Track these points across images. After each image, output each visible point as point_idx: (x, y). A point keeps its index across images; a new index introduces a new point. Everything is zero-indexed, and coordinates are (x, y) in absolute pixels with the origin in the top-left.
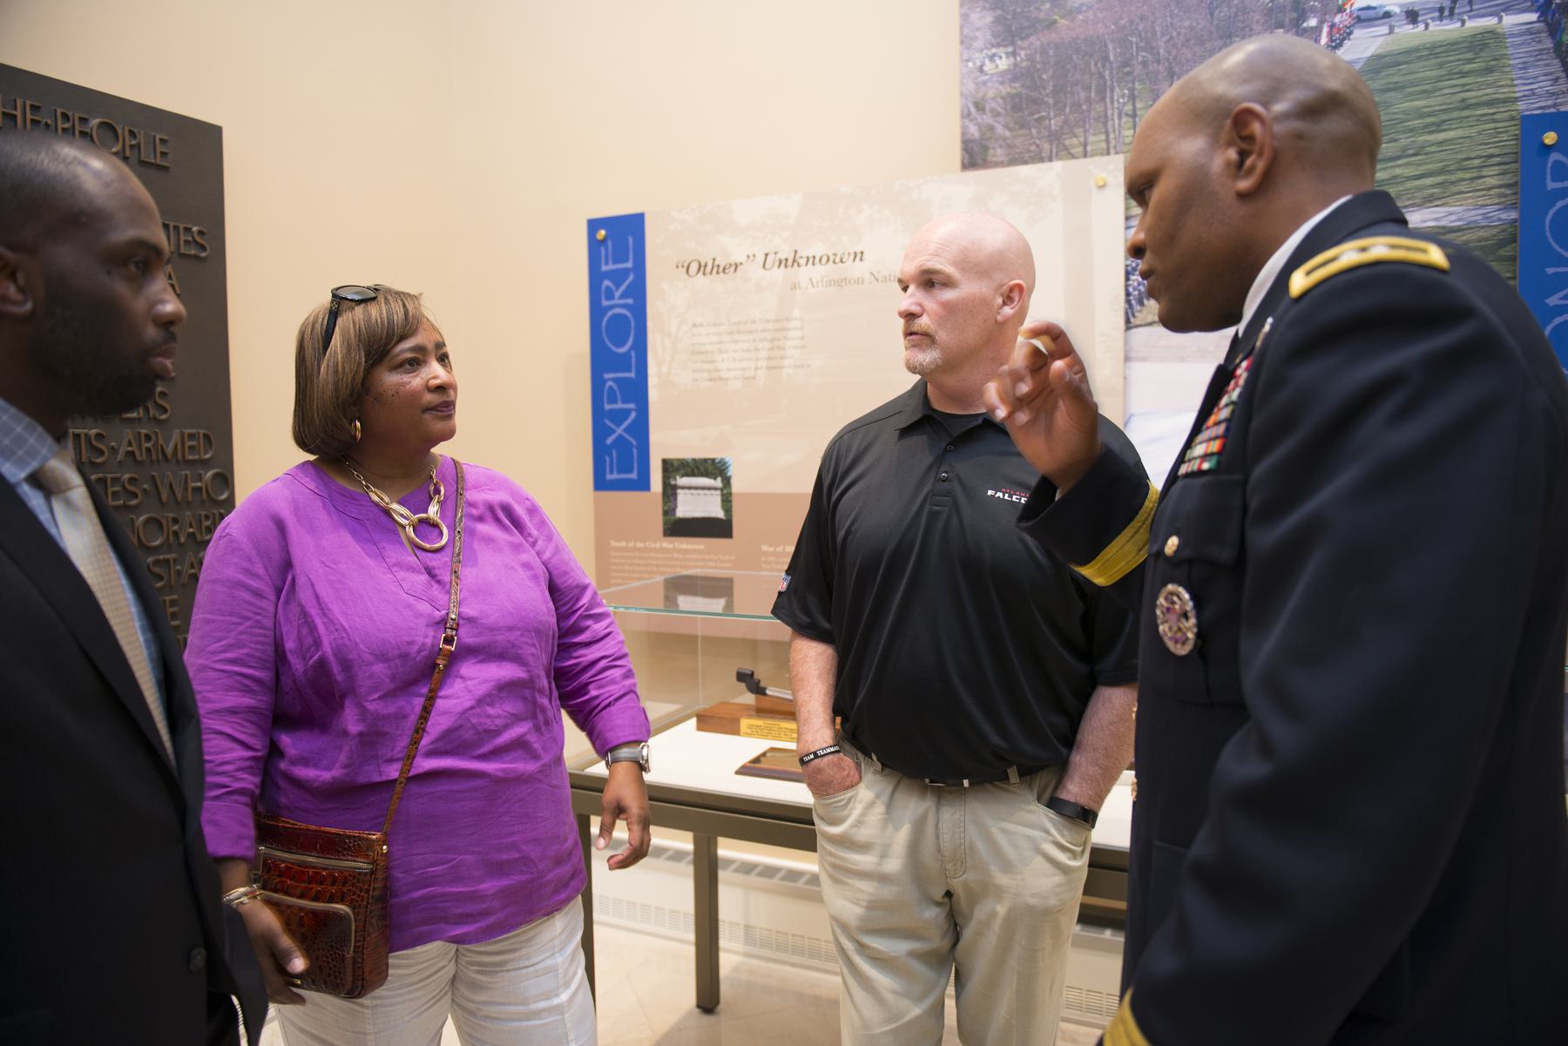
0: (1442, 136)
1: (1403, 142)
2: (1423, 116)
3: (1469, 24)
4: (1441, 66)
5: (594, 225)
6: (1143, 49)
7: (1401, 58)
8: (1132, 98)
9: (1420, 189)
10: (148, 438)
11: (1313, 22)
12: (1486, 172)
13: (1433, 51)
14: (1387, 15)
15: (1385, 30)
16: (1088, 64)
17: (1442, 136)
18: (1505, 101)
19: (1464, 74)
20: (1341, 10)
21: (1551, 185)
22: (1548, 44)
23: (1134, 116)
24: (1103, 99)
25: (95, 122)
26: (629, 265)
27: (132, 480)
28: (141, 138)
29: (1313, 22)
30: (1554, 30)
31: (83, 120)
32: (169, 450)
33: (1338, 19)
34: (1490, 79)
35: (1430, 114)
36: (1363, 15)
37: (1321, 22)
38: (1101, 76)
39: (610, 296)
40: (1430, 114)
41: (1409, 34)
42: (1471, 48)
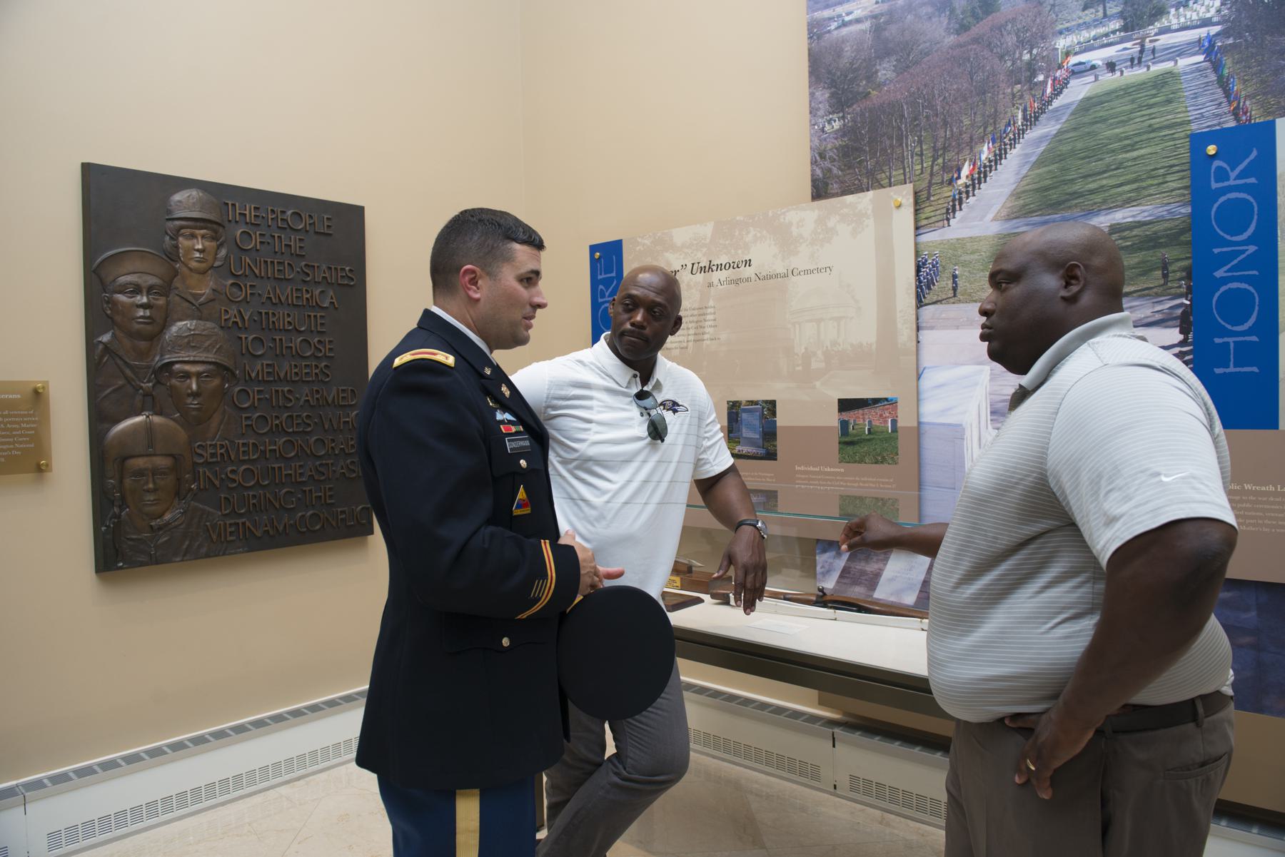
0: (1135, 154)
1: (1107, 160)
2: (1120, 140)
3: (1152, 69)
4: (1133, 101)
5: (593, 249)
6: (927, 107)
7: (1104, 99)
8: (920, 142)
9: (1120, 194)
10: (317, 392)
11: (1041, 78)
12: (1169, 178)
13: (1126, 91)
14: (1093, 67)
15: (1092, 78)
16: (890, 121)
17: (1135, 154)
18: (1181, 124)
19: (1150, 106)
20: (1060, 67)
21: (1214, 185)
22: (1213, 77)
23: (921, 155)
24: (901, 145)
25: (289, 212)
26: (614, 274)
27: (308, 417)
28: (315, 218)
29: (1041, 78)
30: (1217, 67)
31: (283, 212)
32: (330, 400)
33: (1058, 74)
34: (1169, 108)
35: (1127, 138)
36: (1076, 69)
37: (1047, 77)
38: (900, 129)
39: (603, 296)
40: (1127, 138)
41: (1109, 80)
42: (1155, 86)
